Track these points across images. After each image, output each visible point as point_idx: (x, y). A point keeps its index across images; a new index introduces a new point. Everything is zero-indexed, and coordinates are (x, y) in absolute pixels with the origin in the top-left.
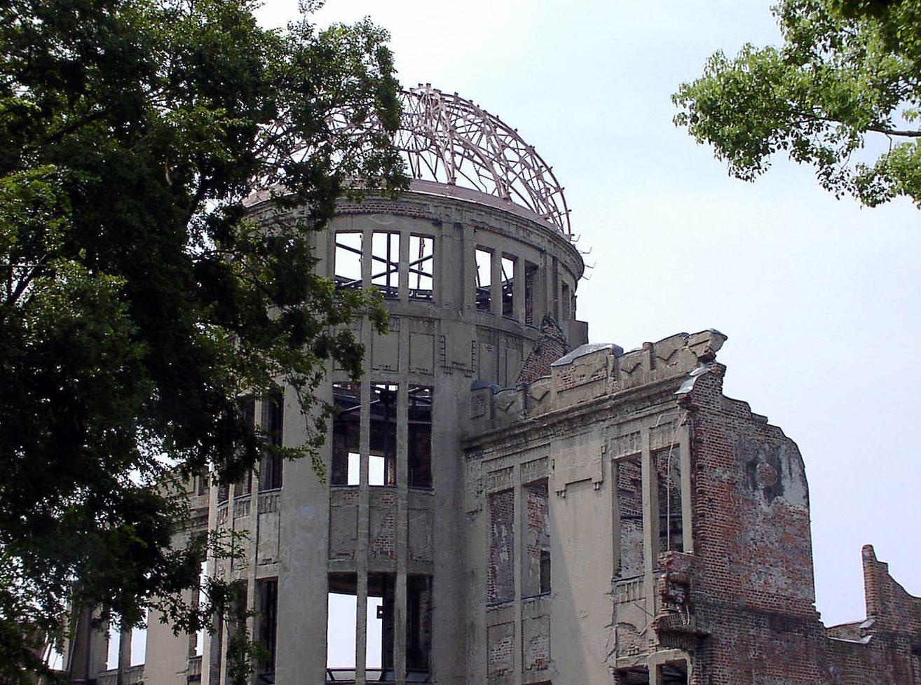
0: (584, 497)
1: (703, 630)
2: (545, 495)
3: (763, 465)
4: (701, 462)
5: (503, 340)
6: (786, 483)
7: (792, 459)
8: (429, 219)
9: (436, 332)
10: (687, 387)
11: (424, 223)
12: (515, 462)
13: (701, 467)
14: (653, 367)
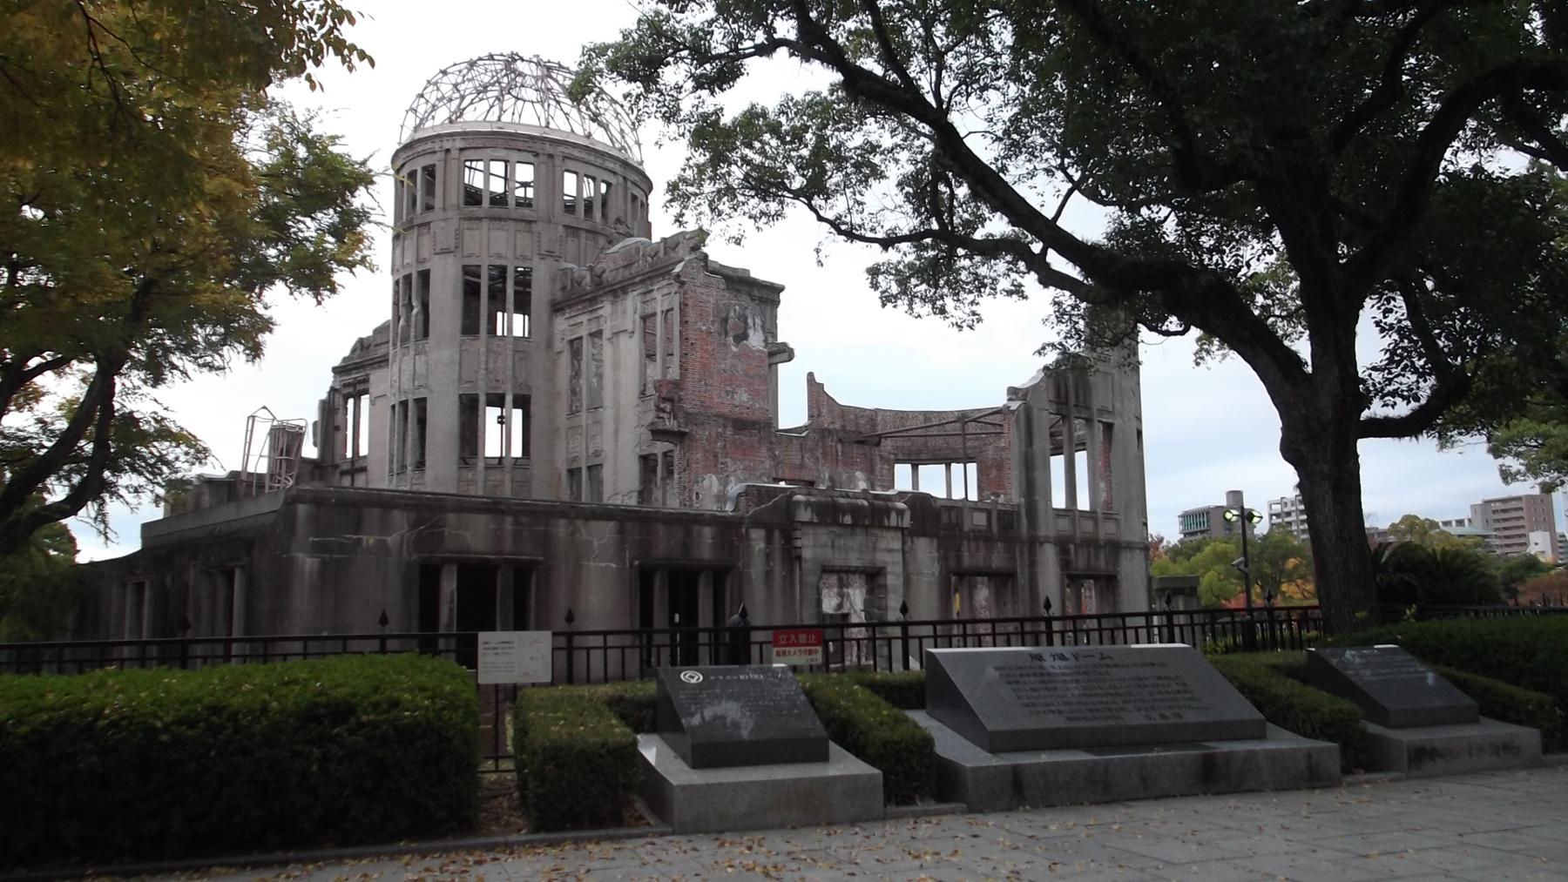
0: (623, 338)
1: (683, 430)
2: (601, 338)
4: (687, 319)
5: (583, 235)
6: (751, 332)
10: (678, 269)
11: (525, 154)
12: (584, 318)
13: (686, 322)
14: (666, 253)
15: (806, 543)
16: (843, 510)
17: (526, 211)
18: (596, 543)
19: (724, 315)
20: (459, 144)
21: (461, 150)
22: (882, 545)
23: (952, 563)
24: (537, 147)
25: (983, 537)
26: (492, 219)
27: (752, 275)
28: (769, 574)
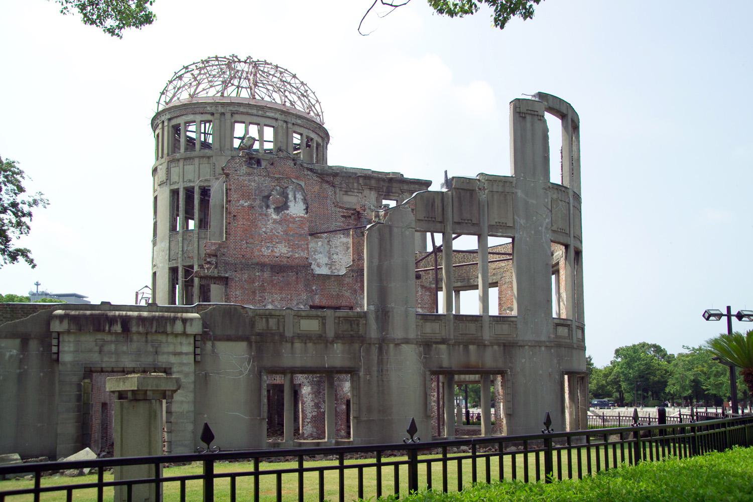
3: (275, 196)
6: (291, 204)
7: (296, 193)
8: (208, 113)
9: (211, 162)
13: (230, 201)
15: (66, 349)
17: (207, 151)
20: (168, 116)
21: (170, 120)
24: (213, 110)
25: (306, 338)
26: (185, 159)
27: (405, 176)
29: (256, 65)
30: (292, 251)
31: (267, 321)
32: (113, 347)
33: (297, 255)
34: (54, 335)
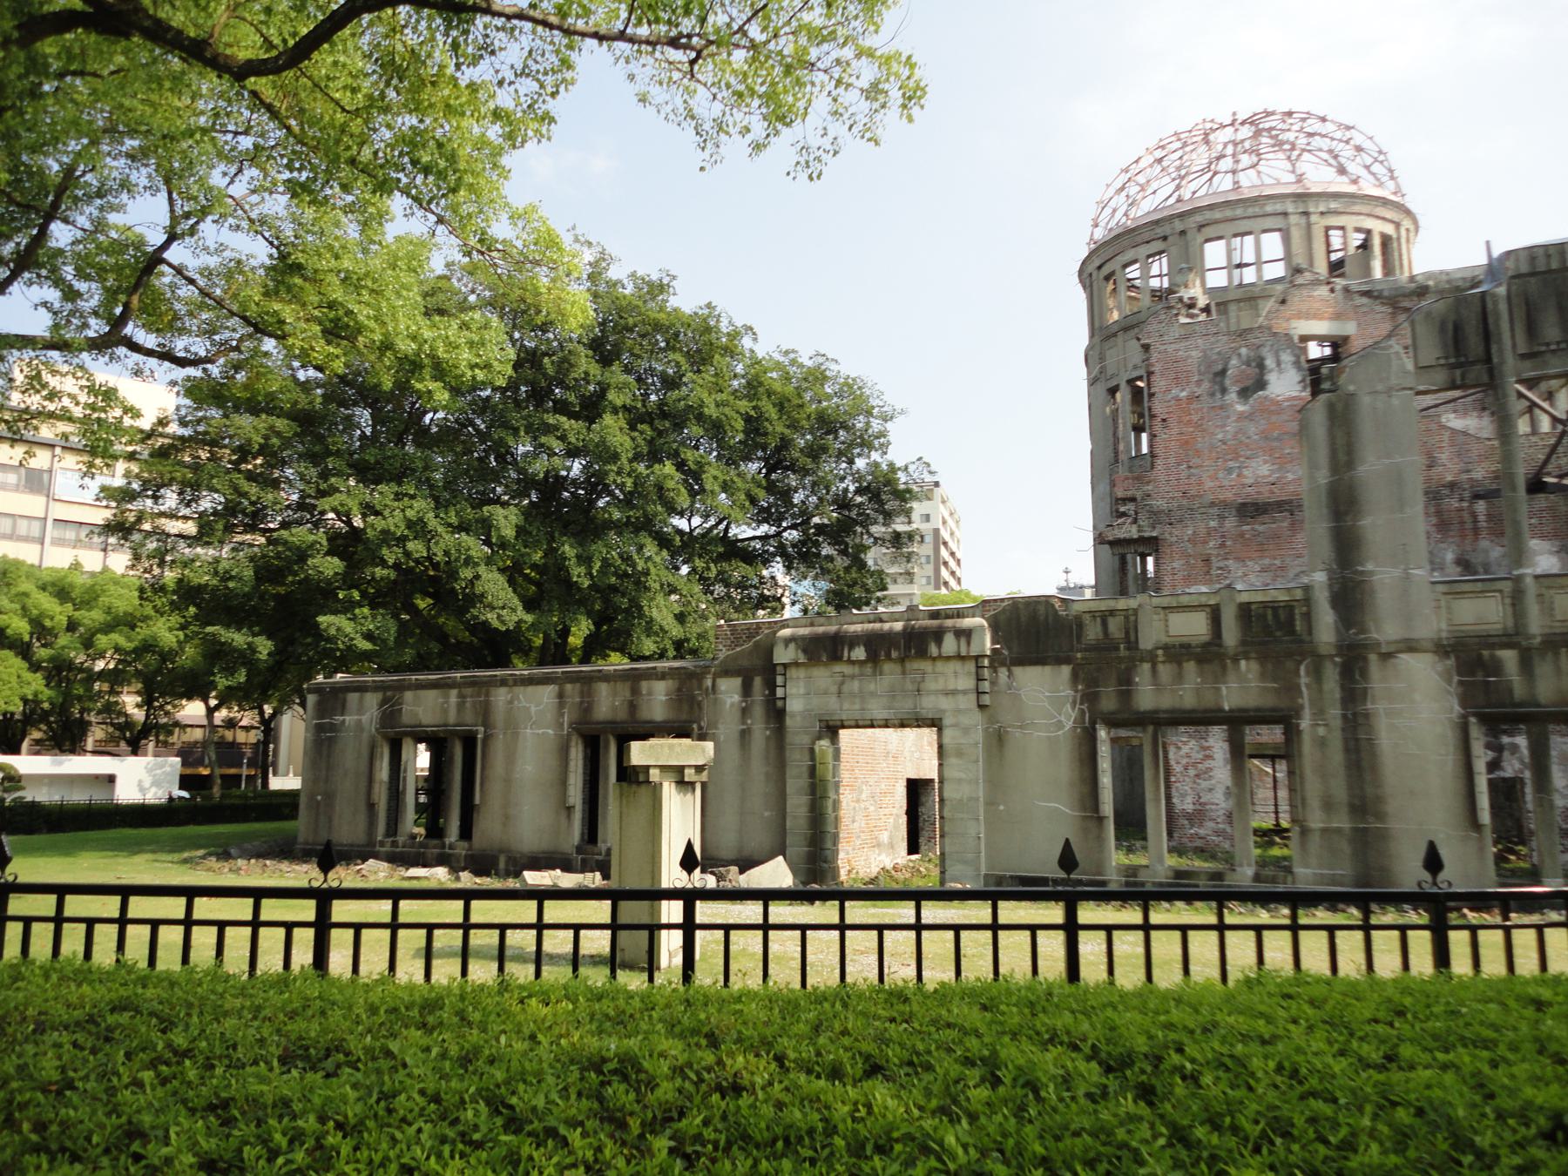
1: (1146, 535)
15: (794, 691)
16: (853, 641)
18: (533, 709)
19: (1220, 367)
20: (1097, 263)
21: (1100, 268)
22: (930, 685)
23: (1108, 703)
24: (1160, 231)
25: (1178, 653)
28: (745, 735)
29: (1250, 121)
30: (1279, 470)
31: (1104, 624)
32: (856, 685)
33: (1290, 476)
34: (780, 669)
